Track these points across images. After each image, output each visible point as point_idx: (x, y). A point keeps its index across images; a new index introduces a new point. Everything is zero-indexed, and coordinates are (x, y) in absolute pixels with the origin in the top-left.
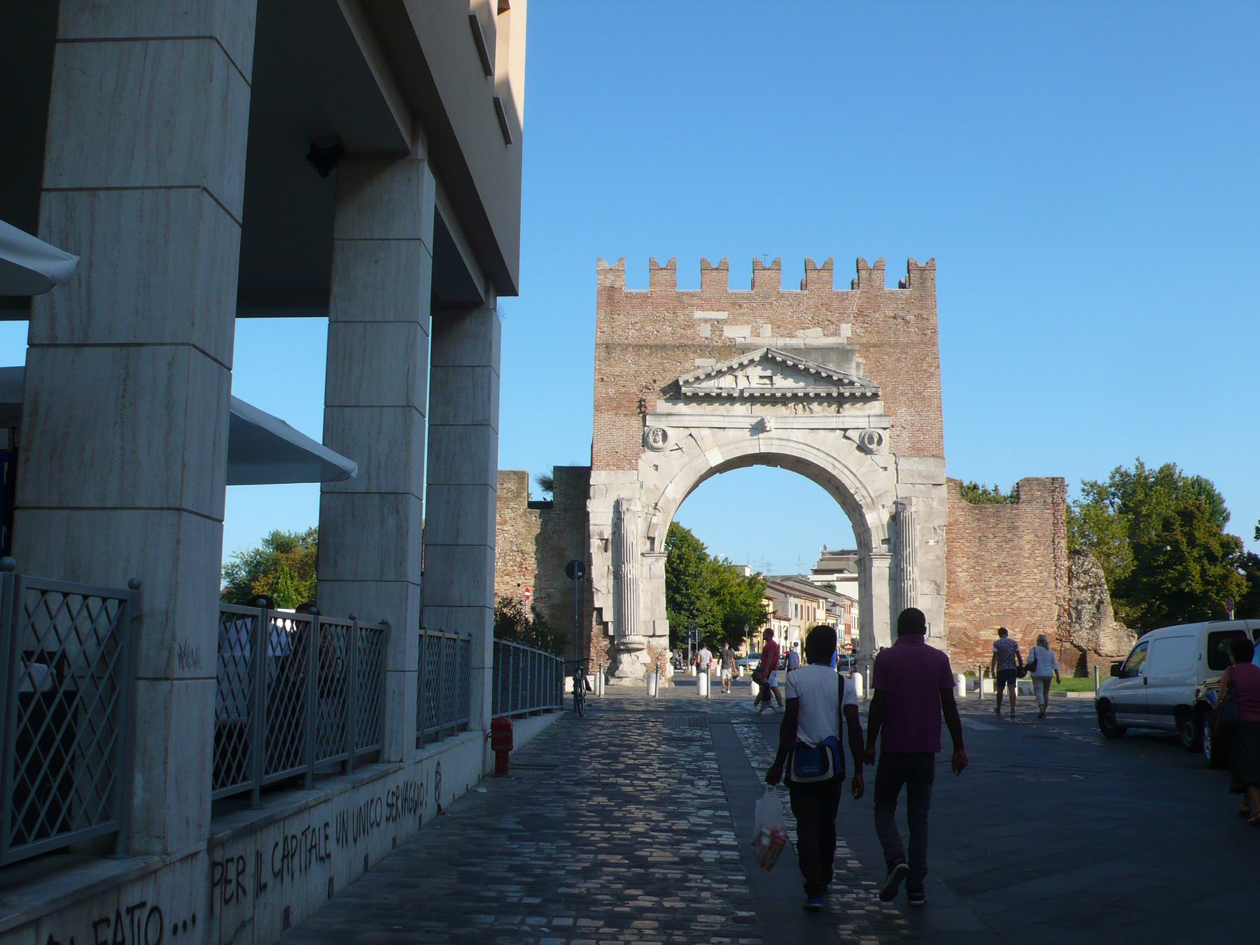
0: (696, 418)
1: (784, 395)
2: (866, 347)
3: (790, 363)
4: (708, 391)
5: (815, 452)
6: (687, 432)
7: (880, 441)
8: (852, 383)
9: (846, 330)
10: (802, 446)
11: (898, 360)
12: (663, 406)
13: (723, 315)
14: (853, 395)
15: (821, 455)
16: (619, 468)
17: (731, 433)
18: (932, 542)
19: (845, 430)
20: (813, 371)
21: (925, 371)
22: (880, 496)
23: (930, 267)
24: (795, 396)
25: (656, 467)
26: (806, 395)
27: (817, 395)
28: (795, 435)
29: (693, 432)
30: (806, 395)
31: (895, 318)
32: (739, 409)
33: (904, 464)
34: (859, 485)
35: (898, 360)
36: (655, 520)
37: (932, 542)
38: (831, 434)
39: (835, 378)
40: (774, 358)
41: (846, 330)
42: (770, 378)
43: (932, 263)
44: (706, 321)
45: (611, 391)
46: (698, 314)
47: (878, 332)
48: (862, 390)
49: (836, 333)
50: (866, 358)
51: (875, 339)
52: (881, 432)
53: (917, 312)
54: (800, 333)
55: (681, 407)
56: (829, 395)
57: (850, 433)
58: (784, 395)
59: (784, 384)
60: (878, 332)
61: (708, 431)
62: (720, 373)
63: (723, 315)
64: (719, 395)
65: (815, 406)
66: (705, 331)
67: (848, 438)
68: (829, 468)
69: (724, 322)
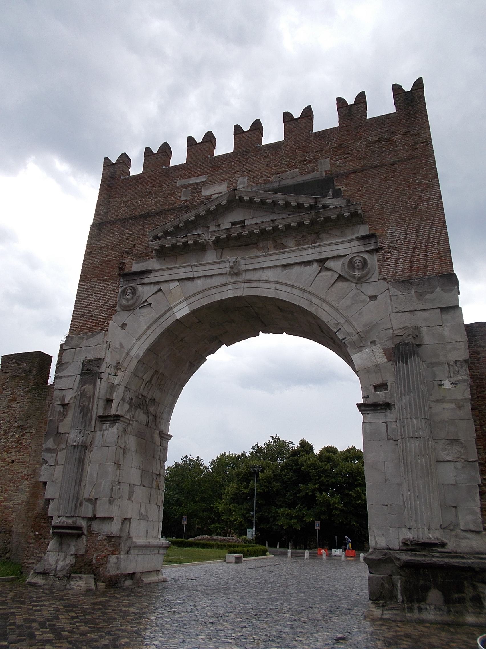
0: (166, 272)
1: (251, 233)
3: (257, 200)
4: (174, 242)
5: (289, 289)
6: (156, 288)
7: (365, 263)
10: (273, 286)
11: (386, 179)
14: (327, 219)
15: (296, 291)
17: (199, 282)
18: (447, 384)
19: (322, 261)
20: (281, 203)
21: (420, 184)
22: (368, 332)
23: (419, 84)
24: (263, 232)
25: (123, 326)
26: (275, 229)
27: (288, 227)
28: (266, 275)
29: (163, 286)
30: (275, 229)
31: (379, 141)
34: (342, 321)
35: (386, 179)
36: (116, 381)
37: (447, 384)
38: (307, 269)
39: (306, 205)
40: (241, 199)
42: (243, 222)
43: (419, 84)
45: (97, 261)
48: (338, 211)
51: (356, 165)
53: (404, 130)
55: (153, 264)
56: (301, 224)
57: (330, 264)
58: (251, 233)
59: (254, 220)
61: (177, 283)
62: (189, 225)
64: (185, 244)
67: (328, 269)
68: (304, 305)
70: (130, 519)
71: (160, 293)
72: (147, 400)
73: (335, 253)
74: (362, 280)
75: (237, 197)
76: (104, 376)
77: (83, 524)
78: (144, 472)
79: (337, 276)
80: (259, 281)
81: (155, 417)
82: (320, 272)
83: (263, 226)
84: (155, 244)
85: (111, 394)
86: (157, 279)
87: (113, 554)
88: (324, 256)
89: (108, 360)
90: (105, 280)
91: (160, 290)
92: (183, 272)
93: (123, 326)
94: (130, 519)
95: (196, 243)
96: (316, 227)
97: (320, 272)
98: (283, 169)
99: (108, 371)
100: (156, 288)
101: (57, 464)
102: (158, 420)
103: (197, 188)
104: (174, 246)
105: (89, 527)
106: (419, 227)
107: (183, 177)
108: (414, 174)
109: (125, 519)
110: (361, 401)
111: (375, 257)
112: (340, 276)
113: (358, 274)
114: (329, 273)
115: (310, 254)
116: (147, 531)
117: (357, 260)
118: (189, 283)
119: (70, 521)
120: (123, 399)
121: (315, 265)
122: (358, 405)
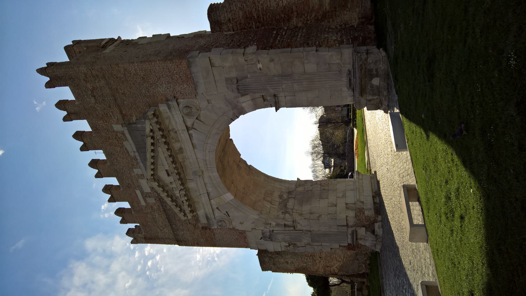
2: (124, 116)
8: (152, 131)
9: (118, 127)
12: (203, 221)
13: (138, 192)
16: (245, 238)
17: (210, 190)
18: (260, 66)
19: (188, 129)
24: (173, 162)
29: (215, 207)
31: (94, 97)
32: (191, 185)
33: (201, 89)
37: (260, 66)
41: (118, 127)
43: (42, 71)
44: (145, 201)
46: (143, 203)
47: (110, 107)
49: (123, 133)
50: (131, 116)
52: (181, 106)
54: (132, 154)
55: (201, 213)
60: (110, 107)
61: (212, 201)
63: (138, 192)
65: (176, 146)
66: (152, 201)
69: (142, 192)
70: (346, 204)
71: (219, 208)
72: (281, 201)
73: (182, 122)
74: (198, 108)
75: (152, 177)
76: (271, 229)
77: (350, 230)
78: (321, 198)
79: (197, 121)
80: (206, 160)
81: (289, 193)
82: (195, 129)
83: (171, 163)
84: (190, 216)
85: (282, 225)
86: (211, 211)
87: (364, 213)
88: (185, 128)
89: (262, 228)
90: (214, 235)
91: (217, 208)
92: (204, 199)
93: (241, 223)
94: (346, 204)
95: (185, 195)
96: (165, 134)
97: (195, 129)
98: (125, 150)
99: (268, 227)
100: (216, 211)
101: (321, 245)
102: (290, 190)
103: (145, 196)
104: (189, 206)
105: (352, 227)
106: (156, 77)
107: (139, 202)
108: (117, 78)
109: (346, 208)
110: (274, 108)
111: (180, 101)
112: (197, 119)
113: (194, 110)
114: (195, 124)
115: (184, 136)
116: (351, 190)
117: (185, 111)
118: (211, 194)
119: (349, 237)
120: (284, 219)
121: (190, 132)
122: (277, 110)
